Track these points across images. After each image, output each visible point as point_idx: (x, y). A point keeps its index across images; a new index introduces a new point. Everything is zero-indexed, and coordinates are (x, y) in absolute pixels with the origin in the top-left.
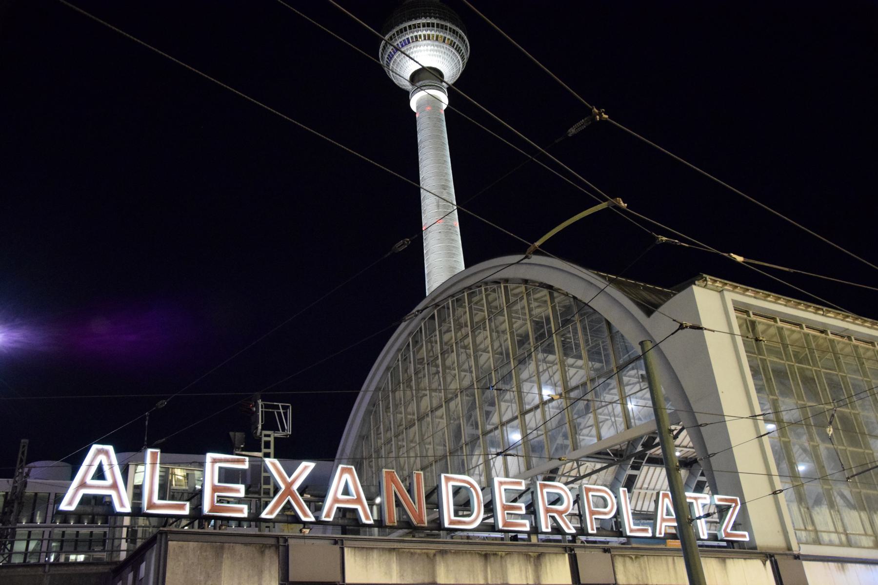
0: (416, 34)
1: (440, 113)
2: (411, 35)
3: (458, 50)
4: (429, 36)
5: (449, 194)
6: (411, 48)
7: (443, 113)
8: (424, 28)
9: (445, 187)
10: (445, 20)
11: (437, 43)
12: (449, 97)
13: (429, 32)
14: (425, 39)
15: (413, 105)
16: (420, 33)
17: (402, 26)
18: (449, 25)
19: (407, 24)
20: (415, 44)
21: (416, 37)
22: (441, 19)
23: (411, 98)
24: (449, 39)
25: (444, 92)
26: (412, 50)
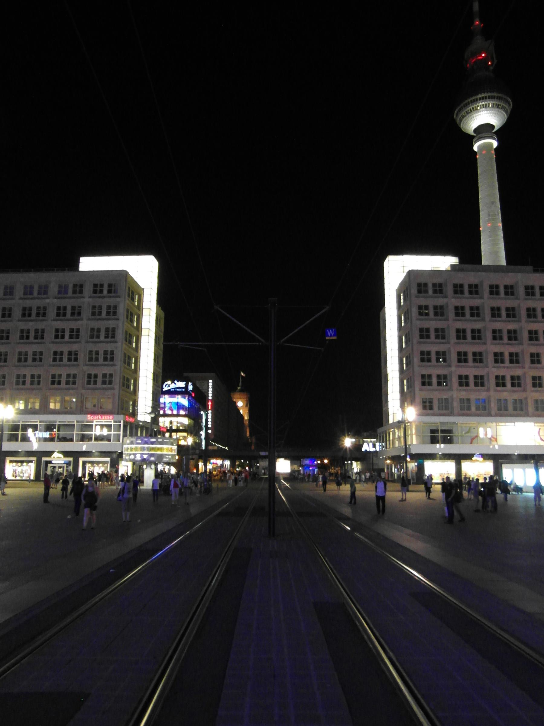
0: (475, 105)
1: (492, 154)
2: (472, 106)
3: (503, 108)
4: (483, 105)
5: (496, 206)
6: (472, 115)
7: (493, 152)
8: (480, 101)
9: (493, 203)
10: (493, 92)
11: (488, 109)
12: (499, 141)
13: (483, 103)
14: (481, 108)
15: (475, 148)
16: (478, 104)
17: (467, 101)
18: (495, 94)
19: (469, 100)
20: (475, 112)
21: (475, 107)
22: (491, 92)
23: (474, 144)
24: (496, 104)
25: (494, 139)
26: (473, 116)
